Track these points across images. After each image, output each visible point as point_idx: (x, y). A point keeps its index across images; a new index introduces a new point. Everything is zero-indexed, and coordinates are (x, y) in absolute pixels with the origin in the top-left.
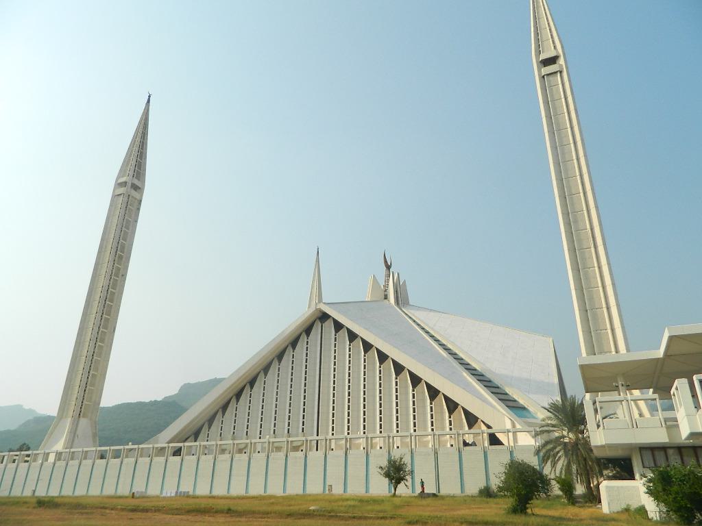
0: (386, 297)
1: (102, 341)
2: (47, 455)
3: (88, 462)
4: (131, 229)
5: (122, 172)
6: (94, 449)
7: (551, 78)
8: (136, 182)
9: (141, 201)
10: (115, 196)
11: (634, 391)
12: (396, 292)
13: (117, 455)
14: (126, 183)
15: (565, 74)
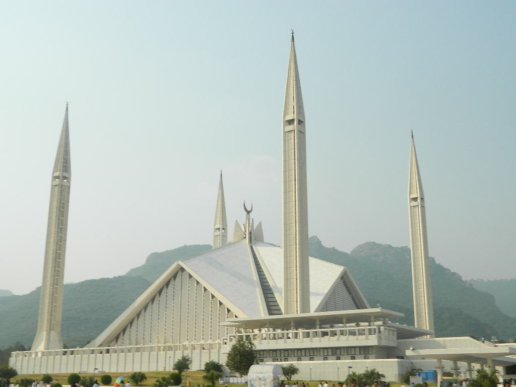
0: (245, 238)
1: (57, 285)
2: (37, 353)
3: (58, 357)
4: (65, 209)
5: (55, 169)
6: (60, 350)
7: (289, 134)
8: (66, 175)
9: (70, 187)
10: (53, 186)
11: (255, 330)
12: (250, 233)
13: (72, 353)
14: (59, 176)
15: (296, 132)
